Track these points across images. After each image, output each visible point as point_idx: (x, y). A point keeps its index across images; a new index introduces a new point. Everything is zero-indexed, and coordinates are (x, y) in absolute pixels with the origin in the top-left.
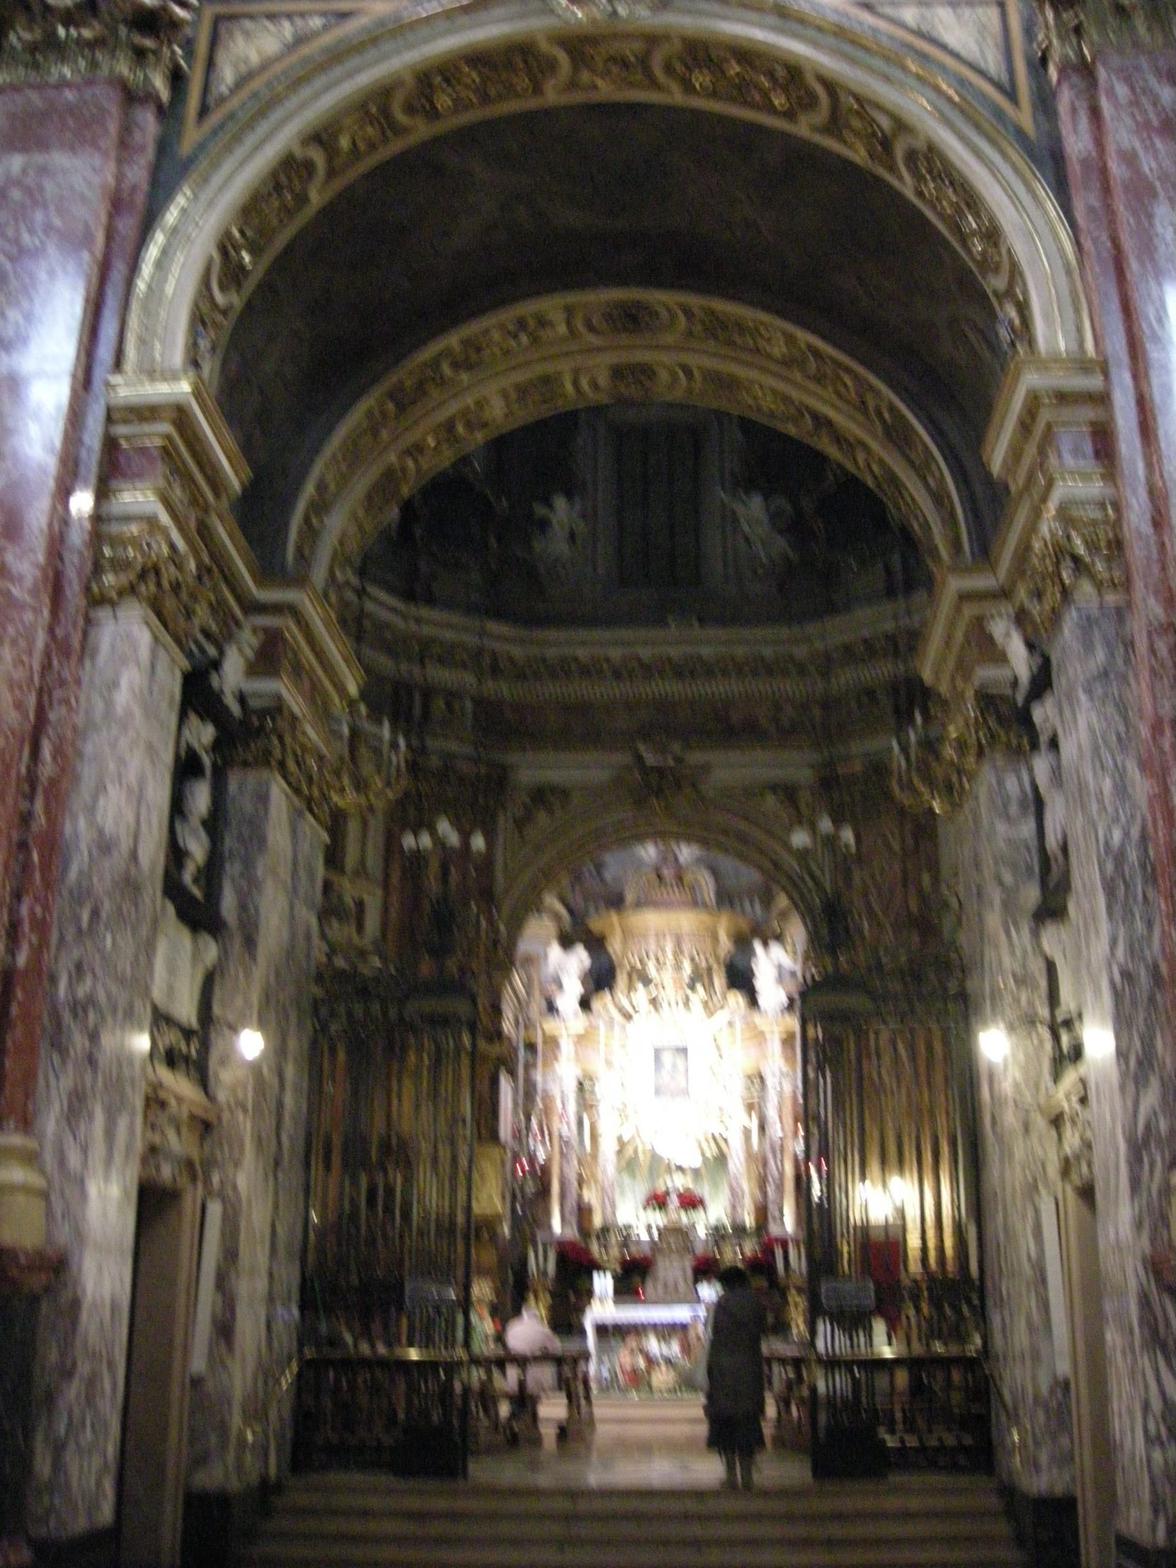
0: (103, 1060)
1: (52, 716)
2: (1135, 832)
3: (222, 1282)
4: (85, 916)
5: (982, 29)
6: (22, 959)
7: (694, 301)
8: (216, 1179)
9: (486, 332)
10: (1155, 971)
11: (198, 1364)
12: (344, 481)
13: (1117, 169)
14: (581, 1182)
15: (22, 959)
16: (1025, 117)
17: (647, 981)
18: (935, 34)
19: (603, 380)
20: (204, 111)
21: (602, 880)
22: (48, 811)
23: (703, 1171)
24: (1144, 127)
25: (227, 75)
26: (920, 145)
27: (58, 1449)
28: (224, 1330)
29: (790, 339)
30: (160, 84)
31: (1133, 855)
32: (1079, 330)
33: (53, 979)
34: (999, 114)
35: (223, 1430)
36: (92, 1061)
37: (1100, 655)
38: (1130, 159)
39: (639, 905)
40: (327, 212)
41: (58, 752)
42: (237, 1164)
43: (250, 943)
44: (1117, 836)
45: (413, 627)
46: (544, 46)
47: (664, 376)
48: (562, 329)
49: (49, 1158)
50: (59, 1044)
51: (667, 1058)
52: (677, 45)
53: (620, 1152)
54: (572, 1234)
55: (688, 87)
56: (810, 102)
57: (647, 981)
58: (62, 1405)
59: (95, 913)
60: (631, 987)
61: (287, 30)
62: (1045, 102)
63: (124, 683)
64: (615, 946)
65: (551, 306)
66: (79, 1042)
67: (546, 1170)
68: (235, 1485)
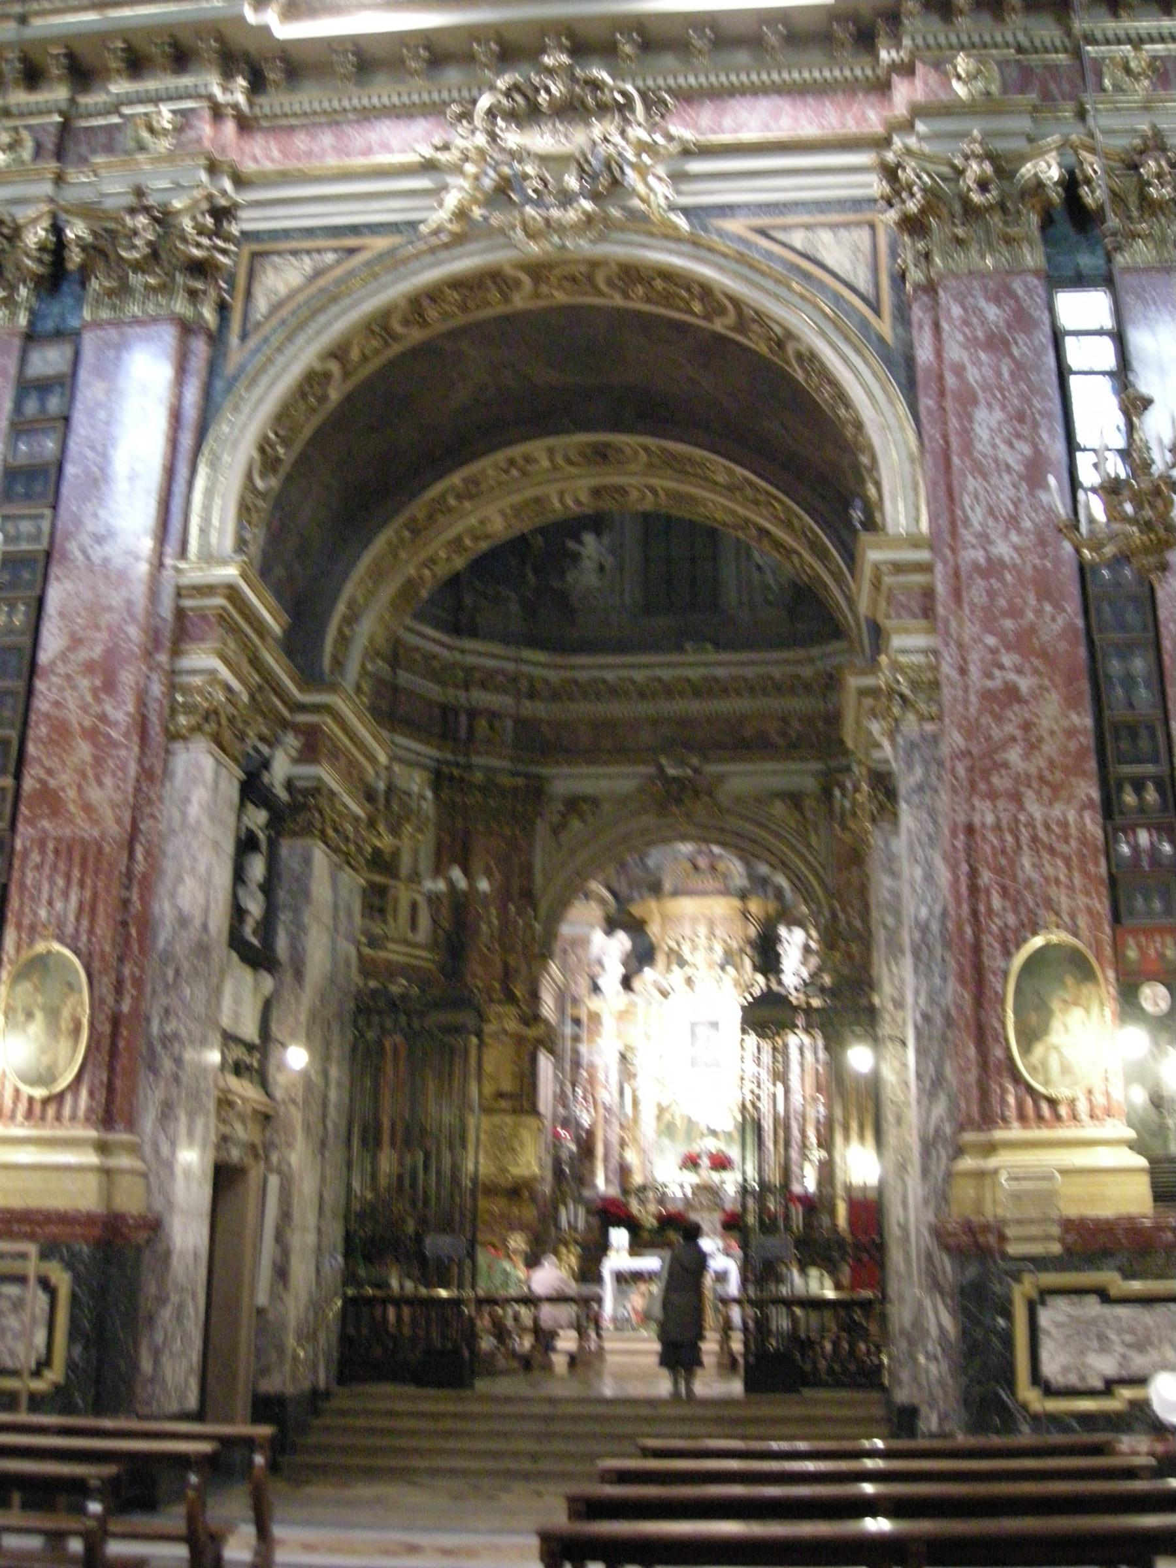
0: (185, 1078)
1: (142, 826)
2: (938, 909)
3: (280, 1238)
4: (170, 973)
5: (856, 249)
6: (126, 1007)
7: (651, 442)
8: (274, 1158)
9: (483, 471)
10: (947, 1016)
11: (262, 1299)
12: (371, 594)
13: (951, 380)
14: (623, 1144)
15: (126, 1007)
16: (885, 327)
17: (682, 963)
18: (819, 256)
19: (584, 498)
20: (244, 337)
21: (644, 865)
22: (142, 898)
24: (971, 343)
25: (261, 304)
26: (803, 349)
27: (156, 1354)
28: (281, 1273)
29: (730, 472)
30: (209, 315)
31: (935, 927)
32: (917, 509)
33: (148, 1020)
34: (865, 325)
35: (280, 1348)
36: (176, 1079)
37: (919, 772)
38: (959, 370)
39: (676, 893)
40: (348, 399)
41: (148, 854)
42: (290, 1145)
43: (299, 975)
44: (924, 912)
45: (458, 656)
46: (509, 271)
47: (634, 494)
48: (546, 463)
49: (147, 1149)
50: (154, 1069)
52: (615, 268)
53: (659, 1118)
54: (614, 1191)
55: (626, 296)
56: (723, 312)
57: (682, 963)
58: (159, 1322)
59: (177, 972)
61: (308, 264)
62: (902, 316)
63: (195, 799)
64: (654, 930)
65: (537, 448)
66: (167, 1065)
67: (590, 1133)
68: (290, 1390)
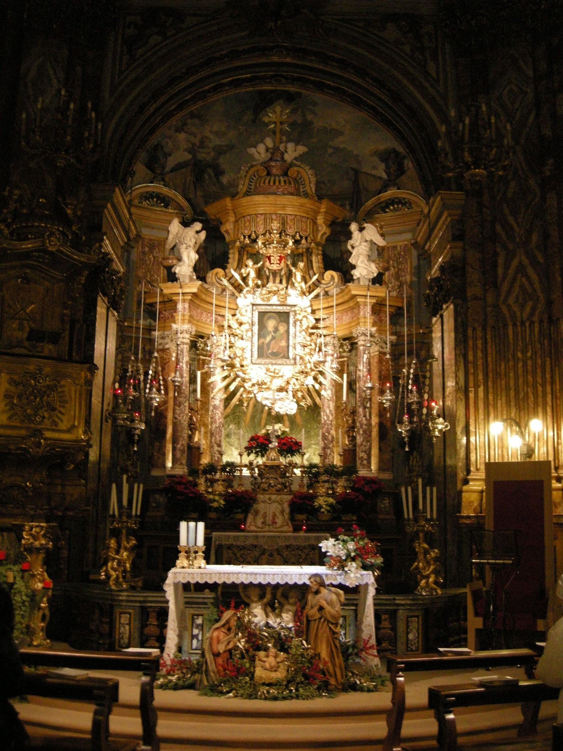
14: (192, 427)
17: (256, 257)
21: (218, 181)
23: (299, 420)
39: (248, 193)
51: (271, 324)
53: (228, 400)
54: (181, 471)
57: (256, 257)
60: (240, 265)
64: (228, 227)
67: (161, 415)
